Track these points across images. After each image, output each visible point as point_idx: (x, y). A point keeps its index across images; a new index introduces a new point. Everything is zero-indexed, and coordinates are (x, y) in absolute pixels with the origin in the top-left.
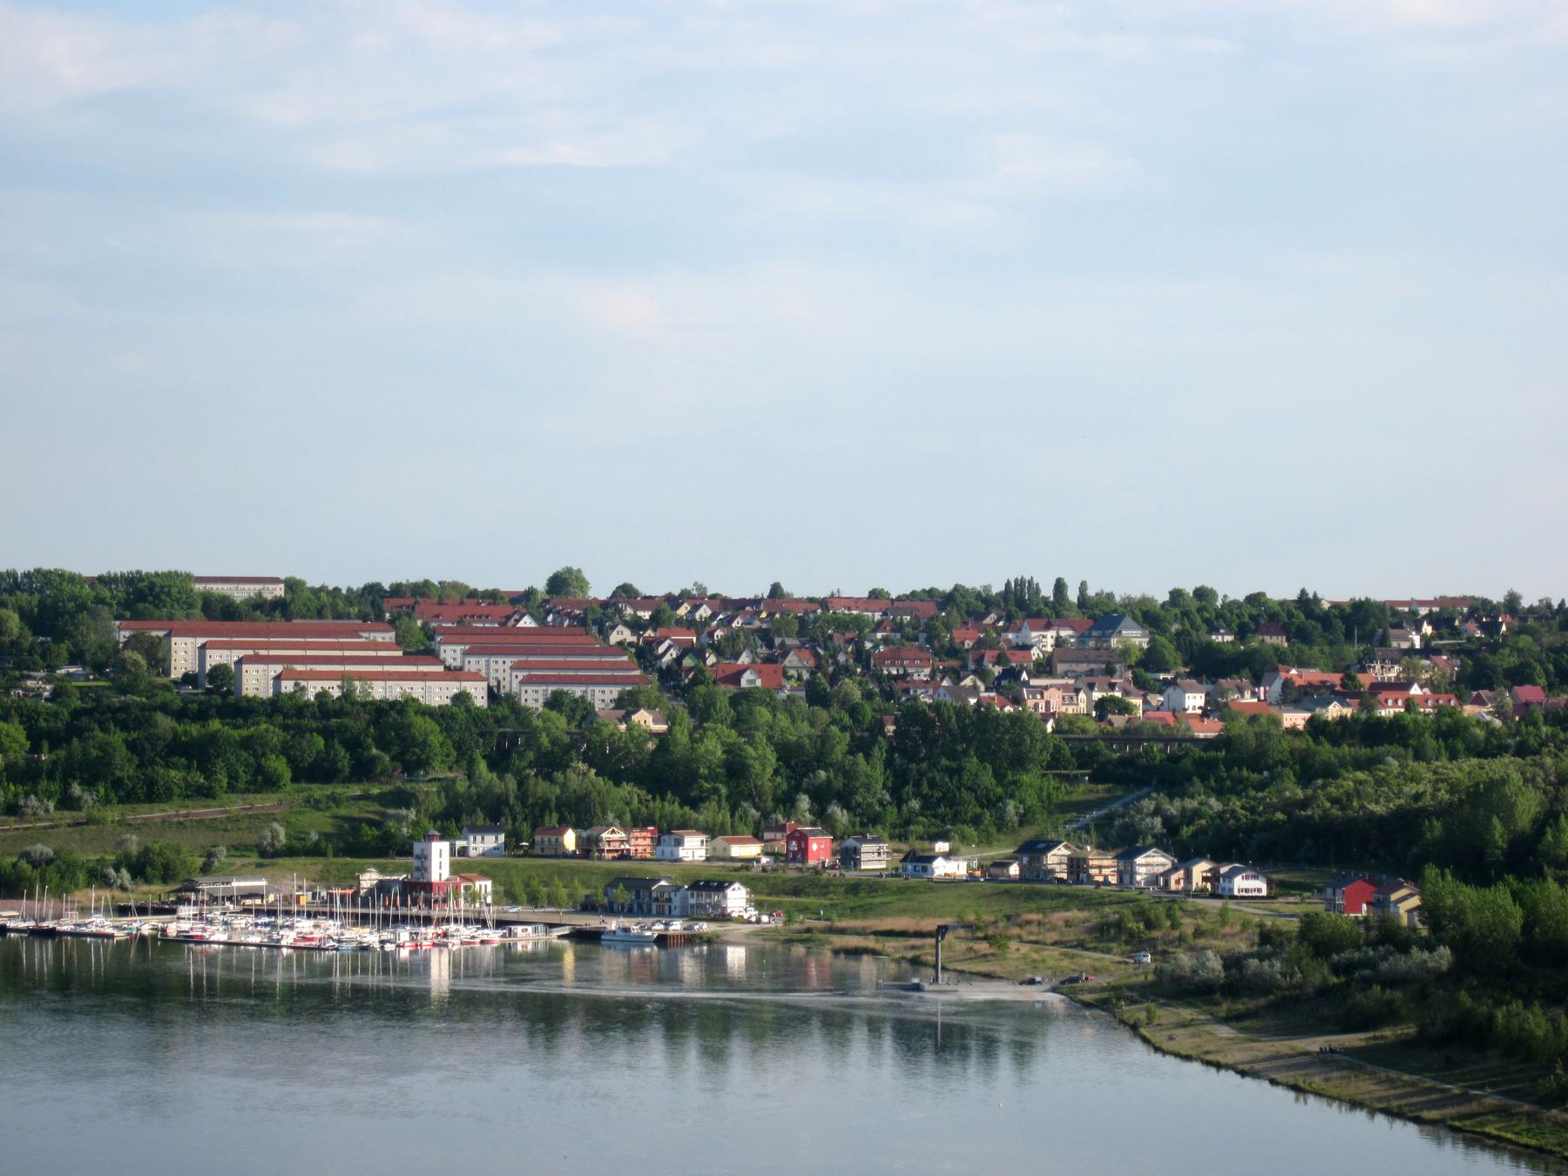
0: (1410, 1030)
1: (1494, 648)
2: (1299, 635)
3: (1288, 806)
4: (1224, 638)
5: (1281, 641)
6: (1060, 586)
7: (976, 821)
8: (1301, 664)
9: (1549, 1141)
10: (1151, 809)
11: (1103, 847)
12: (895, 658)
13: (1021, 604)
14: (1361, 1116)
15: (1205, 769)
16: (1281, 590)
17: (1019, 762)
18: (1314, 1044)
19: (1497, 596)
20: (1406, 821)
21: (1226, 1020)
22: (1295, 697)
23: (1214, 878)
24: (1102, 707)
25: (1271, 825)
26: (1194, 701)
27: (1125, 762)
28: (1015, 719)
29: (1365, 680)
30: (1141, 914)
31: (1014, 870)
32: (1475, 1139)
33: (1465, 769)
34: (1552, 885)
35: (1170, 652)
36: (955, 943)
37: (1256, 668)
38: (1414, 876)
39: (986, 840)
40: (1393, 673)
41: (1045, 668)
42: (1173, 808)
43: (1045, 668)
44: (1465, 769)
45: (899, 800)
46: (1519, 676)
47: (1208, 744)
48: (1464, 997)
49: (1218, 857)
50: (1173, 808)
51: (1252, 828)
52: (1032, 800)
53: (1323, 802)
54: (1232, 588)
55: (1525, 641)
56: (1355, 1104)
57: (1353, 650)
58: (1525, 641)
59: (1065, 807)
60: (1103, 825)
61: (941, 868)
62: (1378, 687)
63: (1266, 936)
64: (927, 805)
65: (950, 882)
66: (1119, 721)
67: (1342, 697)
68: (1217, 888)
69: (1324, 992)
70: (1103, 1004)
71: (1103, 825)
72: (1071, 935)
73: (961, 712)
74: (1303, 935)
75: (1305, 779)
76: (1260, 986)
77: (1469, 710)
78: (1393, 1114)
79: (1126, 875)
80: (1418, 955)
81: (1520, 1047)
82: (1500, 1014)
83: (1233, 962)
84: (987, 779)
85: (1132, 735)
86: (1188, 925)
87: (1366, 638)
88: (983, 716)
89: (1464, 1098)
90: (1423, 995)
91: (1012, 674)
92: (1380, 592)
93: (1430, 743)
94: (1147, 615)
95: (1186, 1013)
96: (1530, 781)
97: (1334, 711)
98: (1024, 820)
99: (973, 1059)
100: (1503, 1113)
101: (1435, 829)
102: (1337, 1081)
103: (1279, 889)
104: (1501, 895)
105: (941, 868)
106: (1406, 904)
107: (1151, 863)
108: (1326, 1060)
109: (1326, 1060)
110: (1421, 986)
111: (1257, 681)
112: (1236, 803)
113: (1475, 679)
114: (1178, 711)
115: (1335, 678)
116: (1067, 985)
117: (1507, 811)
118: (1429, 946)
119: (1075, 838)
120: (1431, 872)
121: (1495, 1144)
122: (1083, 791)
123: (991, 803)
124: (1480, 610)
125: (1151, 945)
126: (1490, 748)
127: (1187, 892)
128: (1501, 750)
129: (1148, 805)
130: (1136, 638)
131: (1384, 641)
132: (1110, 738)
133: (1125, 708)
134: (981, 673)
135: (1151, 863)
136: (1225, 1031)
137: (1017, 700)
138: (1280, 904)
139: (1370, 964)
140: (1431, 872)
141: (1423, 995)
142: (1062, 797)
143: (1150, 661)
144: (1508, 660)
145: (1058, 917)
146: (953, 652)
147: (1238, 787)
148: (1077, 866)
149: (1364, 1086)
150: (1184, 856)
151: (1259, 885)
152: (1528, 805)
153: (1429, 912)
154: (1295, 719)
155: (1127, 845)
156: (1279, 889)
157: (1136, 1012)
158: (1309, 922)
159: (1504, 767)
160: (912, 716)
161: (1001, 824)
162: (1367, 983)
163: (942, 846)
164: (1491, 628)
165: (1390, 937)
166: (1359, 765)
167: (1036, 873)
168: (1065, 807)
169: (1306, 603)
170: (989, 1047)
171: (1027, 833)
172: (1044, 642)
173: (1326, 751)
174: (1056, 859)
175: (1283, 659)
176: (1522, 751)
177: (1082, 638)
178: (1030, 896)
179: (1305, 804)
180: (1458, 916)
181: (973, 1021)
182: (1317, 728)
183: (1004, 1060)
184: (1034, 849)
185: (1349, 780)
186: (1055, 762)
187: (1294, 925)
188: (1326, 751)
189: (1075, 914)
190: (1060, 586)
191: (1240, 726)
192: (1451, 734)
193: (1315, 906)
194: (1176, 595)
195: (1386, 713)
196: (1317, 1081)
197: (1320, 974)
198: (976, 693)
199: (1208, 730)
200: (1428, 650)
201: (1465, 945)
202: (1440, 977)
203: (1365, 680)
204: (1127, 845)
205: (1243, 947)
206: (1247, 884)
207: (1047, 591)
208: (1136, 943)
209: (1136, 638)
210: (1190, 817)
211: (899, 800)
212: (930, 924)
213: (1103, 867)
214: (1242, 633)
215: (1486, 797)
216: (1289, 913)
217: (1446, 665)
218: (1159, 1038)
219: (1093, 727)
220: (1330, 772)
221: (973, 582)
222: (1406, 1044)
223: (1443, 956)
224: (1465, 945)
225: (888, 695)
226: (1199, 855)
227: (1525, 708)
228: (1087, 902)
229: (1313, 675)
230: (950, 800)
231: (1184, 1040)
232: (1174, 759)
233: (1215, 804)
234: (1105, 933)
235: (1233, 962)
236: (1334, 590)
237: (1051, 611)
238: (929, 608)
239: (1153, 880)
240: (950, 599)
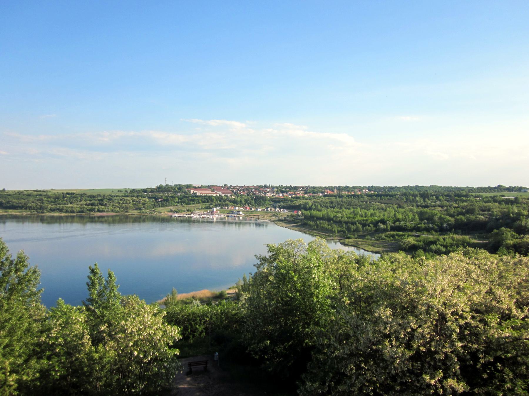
0: (300, 224)
1: (307, 190)
2: (290, 189)
3: (289, 204)
4: (284, 190)
5: (289, 190)
6: (269, 185)
7: (262, 206)
8: (290, 192)
9: (313, 233)
10: (277, 204)
11: (273, 208)
12: (255, 191)
13: (266, 187)
14: (296, 231)
15: (282, 201)
16: (289, 185)
17: (266, 200)
18: (292, 225)
19: (308, 186)
20: (300, 205)
21: (285, 223)
22: (290, 195)
23: (283, 210)
24: (273, 196)
25: (288, 206)
26: (281, 195)
27: (275, 200)
28: (265, 197)
29: (296, 193)
30: (277, 214)
31: (265, 210)
32: (306, 233)
33: (305, 201)
34: (313, 211)
35: (279, 191)
36: (260, 217)
37: (287, 192)
38: (301, 210)
39: (263, 207)
40: (298, 193)
41: (268, 192)
42: (279, 204)
43: (268, 192)
44: (305, 201)
45: (255, 204)
46: (310, 193)
47: (282, 199)
48: (305, 221)
49: (283, 209)
50: (279, 204)
51: (286, 206)
52: (267, 204)
53: (292, 204)
54: (284, 185)
55: (310, 190)
56: (296, 230)
57: (295, 190)
58: (310, 190)
59: (270, 204)
60: (273, 206)
61: (259, 210)
62: (297, 194)
63: (288, 216)
64: (258, 204)
65: (260, 211)
66: (274, 197)
67: (294, 195)
68: (283, 211)
69: (293, 220)
70: (273, 222)
71: (273, 206)
72: (270, 216)
73: (261, 196)
74: (291, 215)
75: (291, 202)
76: (287, 220)
77: (305, 196)
78: (299, 231)
79: (275, 210)
80: (301, 217)
81: (310, 225)
82: (308, 222)
83: (285, 218)
84: (263, 202)
85: (276, 198)
86: (281, 215)
87: (296, 189)
88: (263, 197)
89: (305, 230)
90: (301, 221)
91: (265, 193)
92: (297, 185)
93: (302, 198)
94: (277, 188)
95: (281, 222)
96: (311, 202)
97: (293, 196)
98: (266, 206)
99: (262, 227)
100: (309, 231)
101: (302, 206)
102: (294, 228)
103: (288, 211)
104: (308, 212)
105: (259, 210)
106: (300, 213)
107: (277, 209)
108: (293, 226)
109: (293, 226)
110: (301, 220)
111: (287, 193)
112: (285, 204)
113: (306, 193)
114: (280, 196)
115: (293, 193)
116: (270, 220)
117: (309, 205)
118: (302, 216)
119: (271, 207)
120: (302, 210)
121: (308, 234)
122: (271, 203)
123: (263, 204)
124: (306, 187)
125: (277, 216)
126: (307, 199)
127: (281, 212)
128: (308, 199)
129: (277, 204)
130: (276, 190)
131: (298, 190)
132: (274, 198)
133: (275, 196)
134: (262, 193)
135: (277, 209)
136: (284, 224)
137: (266, 195)
138: (289, 213)
139: (297, 218)
140: (302, 210)
141: (301, 221)
142: (269, 203)
143: (277, 191)
144: (308, 191)
145: (269, 214)
146: (260, 191)
147: (285, 203)
148: (271, 210)
149: (296, 229)
150: (280, 209)
151: (287, 211)
152: (310, 204)
153: (302, 213)
154: (290, 197)
155: (275, 208)
156: (288, 211)
157: (276, 222)
158: (291, 214)
159: (308, 201)
160: (256, 197)
161: (264, 206)
162: (296, 220)
163: (259, 208)
164: (307, 188)
165: (298, 216)
166: (296, 201)
167: (267, 210)
168: (270, 204)
169: (291, 186)
170: (263, 225)
171: (267, 207)
172: (268, 190)
173: (293, 199)
174: (269, 209)
175: (289, 191)
176: (310, 199)
177: (271, 190)
178: (267, 212)
179: (291, 204)
180: (304, 214)
181: (262, 223)
182: (292, 197)
183: (265, 226)
184: (267, 208)
185: (295, 202)
186: (269, 200)
187: (290, 215)
188: (293, 199)
189: (271, 214)
190: (269, 185)
191: (285, 197)
192: (304, 198)
193: (292, 213)
194: (279, 186)
195: (298, 196)
196: (292, 228)
197: (292, 219)
198: (262, 194)
199: (282, 198)
200: (302, 190)
201: (305, 216)
202: (303, 219)
203: (296, 193)
204: (275, 208)
205: (285, 217)
206: (286, 211)
207: (268, 186)
208: (276, 216)
209: (276, 190)
210: (281, 205)
211: (255, 204)
212: (258, 215)
213: (273, 210)
214: (285, 189)
215: (307, 203)
216: (289, 214)
217: (303, 192)
218: (278, 225)
219: (272, 197)
220: (293, 201)
221: (262, 185)
222: (300, 225)
223: (303, 217)
224: (305, 216)
225: (254, 195)
226: (282, 208)
227: (310, 196)
228: (272, 213)
229: (291, 193)
230: (260, 204)
231: (280, 225)
232: (279, 200)
233: (283, 204)
234: (273, 215)
235: (285, 218)
236: (293, 185)
237: (268, 187)
238: (258, 187)
239: (278, 211)
240: (259, 186)
